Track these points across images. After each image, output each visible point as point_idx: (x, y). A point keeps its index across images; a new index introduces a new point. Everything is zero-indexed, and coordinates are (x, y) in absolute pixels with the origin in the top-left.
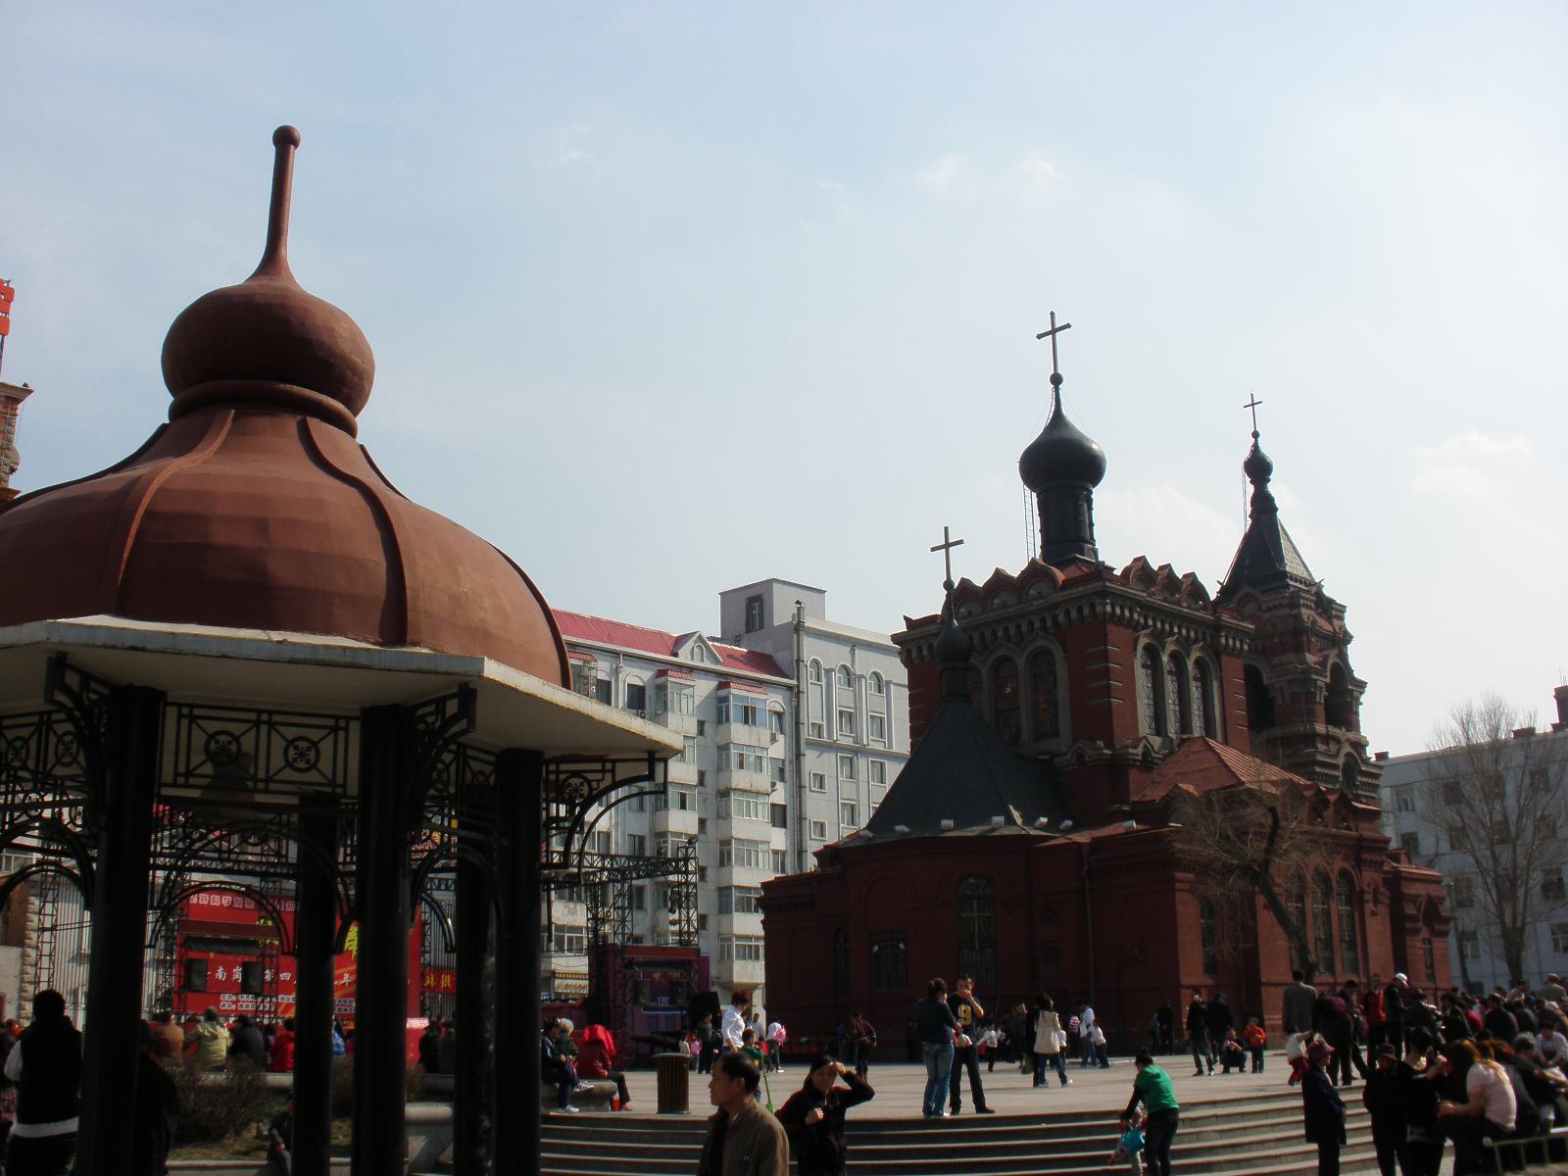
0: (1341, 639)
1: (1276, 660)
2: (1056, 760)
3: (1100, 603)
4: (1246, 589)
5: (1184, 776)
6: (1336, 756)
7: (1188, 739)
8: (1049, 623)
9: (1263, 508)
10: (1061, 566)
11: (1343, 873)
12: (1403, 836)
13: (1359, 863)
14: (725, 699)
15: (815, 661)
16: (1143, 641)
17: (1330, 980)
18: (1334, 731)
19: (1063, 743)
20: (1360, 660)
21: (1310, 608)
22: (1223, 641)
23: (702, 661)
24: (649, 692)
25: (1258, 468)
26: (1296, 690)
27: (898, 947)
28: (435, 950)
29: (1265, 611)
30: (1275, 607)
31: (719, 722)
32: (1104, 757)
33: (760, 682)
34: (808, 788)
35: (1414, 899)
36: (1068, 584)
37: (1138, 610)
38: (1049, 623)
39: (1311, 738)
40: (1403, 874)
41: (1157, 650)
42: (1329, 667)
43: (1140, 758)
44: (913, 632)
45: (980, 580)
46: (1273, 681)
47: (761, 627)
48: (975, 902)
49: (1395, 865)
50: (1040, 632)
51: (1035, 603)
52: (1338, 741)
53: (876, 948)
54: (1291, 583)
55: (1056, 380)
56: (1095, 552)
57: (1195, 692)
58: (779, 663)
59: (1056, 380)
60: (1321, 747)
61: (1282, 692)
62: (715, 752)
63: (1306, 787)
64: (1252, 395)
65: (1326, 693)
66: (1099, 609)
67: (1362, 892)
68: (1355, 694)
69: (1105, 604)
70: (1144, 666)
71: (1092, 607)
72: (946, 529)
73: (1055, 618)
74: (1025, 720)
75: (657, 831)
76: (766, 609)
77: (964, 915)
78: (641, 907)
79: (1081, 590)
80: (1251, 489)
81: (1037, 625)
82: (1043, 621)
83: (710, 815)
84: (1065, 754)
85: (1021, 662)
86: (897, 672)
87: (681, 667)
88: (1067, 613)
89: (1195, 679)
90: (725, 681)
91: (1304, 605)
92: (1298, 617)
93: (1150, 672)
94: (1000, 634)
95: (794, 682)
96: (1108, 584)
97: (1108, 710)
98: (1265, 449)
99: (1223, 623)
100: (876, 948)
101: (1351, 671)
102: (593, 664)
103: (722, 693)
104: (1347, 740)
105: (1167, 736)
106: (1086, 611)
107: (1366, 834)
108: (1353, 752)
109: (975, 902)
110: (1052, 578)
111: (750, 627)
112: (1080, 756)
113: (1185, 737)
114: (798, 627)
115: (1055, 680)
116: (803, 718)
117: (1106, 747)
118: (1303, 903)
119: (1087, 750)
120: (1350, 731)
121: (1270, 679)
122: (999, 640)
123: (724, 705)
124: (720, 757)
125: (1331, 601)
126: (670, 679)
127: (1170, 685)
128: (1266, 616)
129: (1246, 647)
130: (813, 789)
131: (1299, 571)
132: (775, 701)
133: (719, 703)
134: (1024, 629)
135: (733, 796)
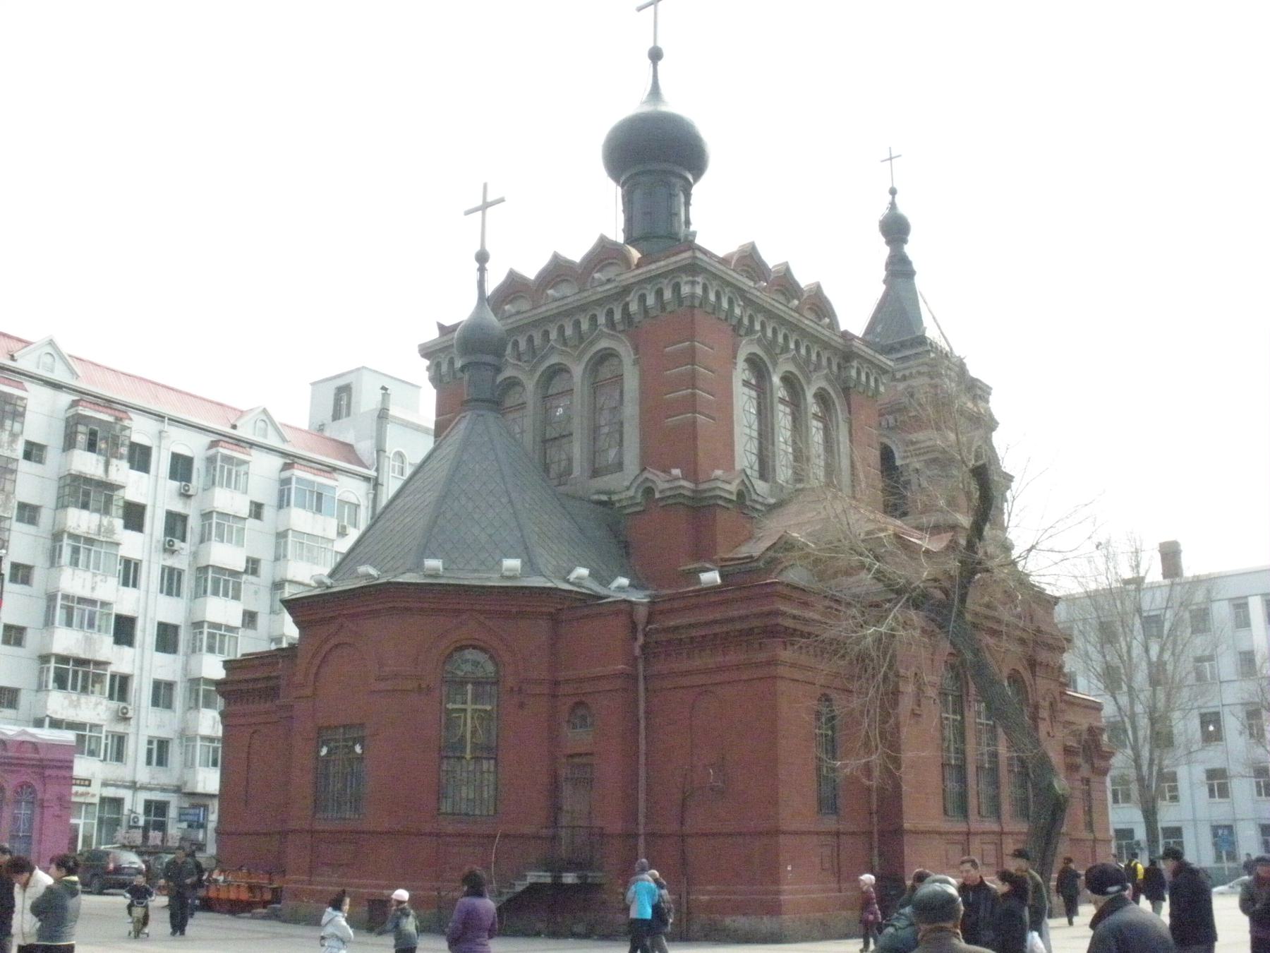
0: (986, 424)
1: (914, 437)
3: (686, 283)
5: (799, 526)
7: (802, 490)
8: (618, 316)
9: (899, 270)
14: (285, 482)
15: (400, 455)
16: (744, 351)
17: (995, 827)
25: (895, 229)
27: (352, 750)
29: (898, 380)
31: (280, 507)
33: (334, 469)
37: (741, 303)
38: (618, 316)
41: (767, 369)
43: (734, 498)
44: (445, 338)
45: (531, 271)
46: (908, 461)
47: (348, 414)
48: (469, 687)
50: (605, 330)
51: (600, 289)
53: (324, 751)
55: (656, 55)
58: (358, 453)
59: (656, 55)
62: (273, 540)
66: (686, 290)
69: (693, 283)
70: (746, 383)
71: (676, 288)
72: (485, 186)
74: (578, 450)
76: (354, 400)
77: (450, 706)
78: (169, 706)
80: (886, 251)
81: (602, 320)
82: (610, 313)
84: (628, 488)
85: (578, 370)
87: (239, 442)
95: (372, 473)
97: (691, 431)
98: (903, 209)
99: (855, 350)
100: (324, 751)
102: (126, 423)
103: (286, 474)
106: (668, 295)
110: (626, 259)
111: (336, 416)
112: (649, 492)
113: (799, 486)
114: (383, 415)
117: (685, 478)
121: (904, 458)
122: (552, 342)
124: (277, 545)
126: (221, 450)
128: (901, 386)
134: (585, 326)
135: (287, 584)
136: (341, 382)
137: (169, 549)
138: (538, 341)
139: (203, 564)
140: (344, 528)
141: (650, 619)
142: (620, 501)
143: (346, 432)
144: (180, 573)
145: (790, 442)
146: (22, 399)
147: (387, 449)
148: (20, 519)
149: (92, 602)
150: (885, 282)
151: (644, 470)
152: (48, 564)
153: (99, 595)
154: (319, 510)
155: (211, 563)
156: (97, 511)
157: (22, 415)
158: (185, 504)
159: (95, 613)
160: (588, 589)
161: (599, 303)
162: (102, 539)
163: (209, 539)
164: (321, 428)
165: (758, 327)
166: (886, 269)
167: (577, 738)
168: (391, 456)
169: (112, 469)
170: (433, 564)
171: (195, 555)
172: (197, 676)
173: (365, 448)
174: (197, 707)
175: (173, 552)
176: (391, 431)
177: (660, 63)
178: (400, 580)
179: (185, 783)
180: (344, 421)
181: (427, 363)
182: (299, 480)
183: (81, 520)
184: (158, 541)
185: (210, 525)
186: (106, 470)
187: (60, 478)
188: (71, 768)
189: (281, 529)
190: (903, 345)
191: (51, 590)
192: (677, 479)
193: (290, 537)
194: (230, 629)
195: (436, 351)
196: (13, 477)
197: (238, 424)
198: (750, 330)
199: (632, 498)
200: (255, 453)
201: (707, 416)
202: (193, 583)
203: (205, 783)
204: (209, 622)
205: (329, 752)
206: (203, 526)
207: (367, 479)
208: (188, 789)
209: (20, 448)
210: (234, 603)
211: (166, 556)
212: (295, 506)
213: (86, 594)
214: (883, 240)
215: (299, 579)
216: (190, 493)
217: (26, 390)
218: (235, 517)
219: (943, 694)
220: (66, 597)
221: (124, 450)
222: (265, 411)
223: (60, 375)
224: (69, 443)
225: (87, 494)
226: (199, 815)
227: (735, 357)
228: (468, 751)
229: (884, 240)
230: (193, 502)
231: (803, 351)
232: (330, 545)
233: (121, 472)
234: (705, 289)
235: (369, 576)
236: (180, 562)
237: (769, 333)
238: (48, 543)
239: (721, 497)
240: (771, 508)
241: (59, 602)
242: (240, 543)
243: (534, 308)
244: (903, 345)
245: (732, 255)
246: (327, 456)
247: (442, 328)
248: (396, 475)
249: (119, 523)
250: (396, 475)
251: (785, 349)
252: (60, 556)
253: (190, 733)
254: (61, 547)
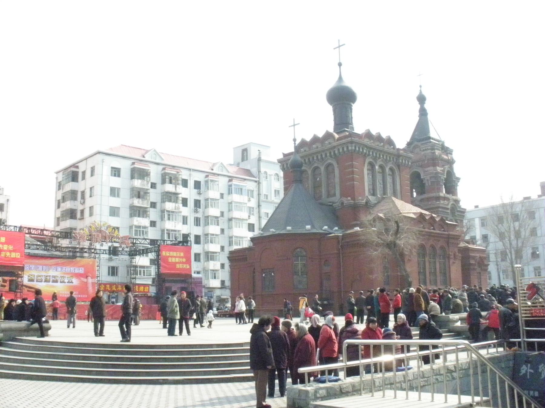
0: (451, 163)
1: (426, 169)
2: (334, 205)
4: (416, 143)
6: (448, 205)
7: (384, 198)
8: (332, 154)
9: (423, 113)
10: (338, 133)
11: (442, 248)
12: (483, 235)
13: (448, 243)
14: (230, 186)
15: (266, 173)
16: (367, 161)
18: (448, 196)
19: (337, 199)
20: (458, 170)
21: (439, 150)
22: (401, 161)
23: (219, 171)
24: (202, 184)
25: (421, 99)
26: (433, 180)
28: (101, 276)
30: (426, 150)
31: (229, 194)
32: (351, 204)
33: (245, 179)
34: (262, 218)
35: (474, 258)
36: (339, 139)
37: (366, 148)
38: (332, 154)
39: (438, 198)
40: (470, 249)
42: (446, 172)
43: (365, 204)
44: (285, 158)
45: (308, 139)
46: (425, 177)
47: (247, 159)
49: (467, 245)
50: (329, 157)
52: (448, 199)
53: (264, 275)
54: (432, 140)
55: (340, 65)
56: (353, 128)
57: (389, 180)
59: (340, 65)
60: (442, 202)
61: (428, 182)
62: (227, 204)
63: (428, 215)
65: (444, 182)
66: (350, 148)
67: (449, 255)
68: (456, 182)
69: (352, 146)
71: (348, 148)
72: (294, 119)
73: (334, 151)
75: (205, 233)
78: (199, 261)
79: (343, 141)
80: (419, 106)
82: (330, 153)
83: (225, 227)
85: (322, 168)
86: (281, 174)
87: (214, 174)
88: (339, 150)
89: (389, 175)
90: (231, 179)
91: (438, 149)
92: (434, 153)
93: (391, 177)
94: (315, 158)
95: (257, 179)
96: (353, 139)
98: (424, 93)
100: (264, 275)
101: (454, 174)
102: (180, 173)
103: (230, 183)
104: (452, 199)
105: (377, 196)
106: (345, 149)
107: (451, 233)
108: (454, 203)
109: (300, 258)
110: (333, 137)
111: (243, 160)
112: (342, 203)
113: (384, 196)
114: (259, 160)
115: (334, 175)
116: (261, 192)
118: (425, 259)
119: (344, 201)
120: (454, 196)
122: (315, 160)
123: (231, 188)
124: (229, 206)
125: (448, 148)
127: (379, 177)
128: (423, 153)
129: (410, 164)
130: (265, 218)
131: (437, 137)
132: (251, 185)
133: (229, 187)
134: (324, 156)
135: (233, 219)
136: (244, 148)
137: (196, 211)
138: (311, 160)
139: (206, 215)
140: (249, 199)
141: (342, 240)
142: (335, 206)
143: (246, 165)
144: (200, 219)
145: (382, 183)
146: (149, 170)
147: (262, 171)
148: (151, 207)
149: (175, 231)
150: (419, 116)
151: (341, 198)
152: (160, 220)
153: (177, 229)
154: (242, 194)
155: (210, 215)
156: (174, 202)
157: (149, 175)
158: (200, 196)
159: (176, 234)
160: (328, 231)
161: (327, 150)
162: (176, 211)
163: (208, 207)
164: (238, 165)
165: (371, 153)
166: (419, 112)
167: (326, 269)
168: (263, 173)
169: (177, 189)
170: (289, 228)
171: (204, 213)
172: (207, 251)
173: (254, 171)
174: (208, 260)
175: (197, 212)
176: (262, 164)
177: (341, 67)
178: (281, 233)
179: (206, 284)
180: (245, 162)
181: (280, 164)
182: (234, 185)
183: (169, 206)
184: (192, 209)
185: (208, 202)
186: (176, 189)
187: (162, 193)
188: (202, 283)
189: (230, 201)
190: (423, 140)
191: (162, 228)
192: (349, 200)
193: (233, 204)
194: (217, 235)
195: (282, 162)
196: (149, 195)
197: (214, 169)
198: (369, 155)
199: (339, 205)
200: (220, 177)
201: (357, 182)
202: (204, 222)
203: (212, 284)
204: (210, 234)
205: (265, 275)
206: (206, 203)
207: (256, 181)
208: (207, 286)
209: (150, 185)
210: (218, 226)
211: (195, 213)
212: (234, 193)
213: (173, 228)
214: (418, 103)
215: (237, 217)
216: (201, 193)
217: (150, 167)
218: (215, 199)
219: (419, 254)
220: (167, 230)
221: (180, 182)
222: (222, 163)
223: (158, 161)
224: (163, 182)
225: (170, 197)
226: (211, 294)
227: (364, 164)
228: (300, 273)
229: (418, 103)
230: (202, 196)
231: (385, 157)
232: (246, 205)
233: (180, 189)
234: (355, 147)
235: (272, 231)
236: (199, 215)
237: (374, 155)
238: (160, 214)
239: (360, 204)
240: (376, 205)
241: (166, 232)
242: (218, 207)
243: (309, 150)
244: (423, 140)
245: (363, 134)
246: (242, 175)
247: (283, 154)
248: (265, 179)
249: (181, 205)
250: (265, 179)
251: (379, 158)
252: (164, 217)
253: (206, 269)
254: (164, 215)
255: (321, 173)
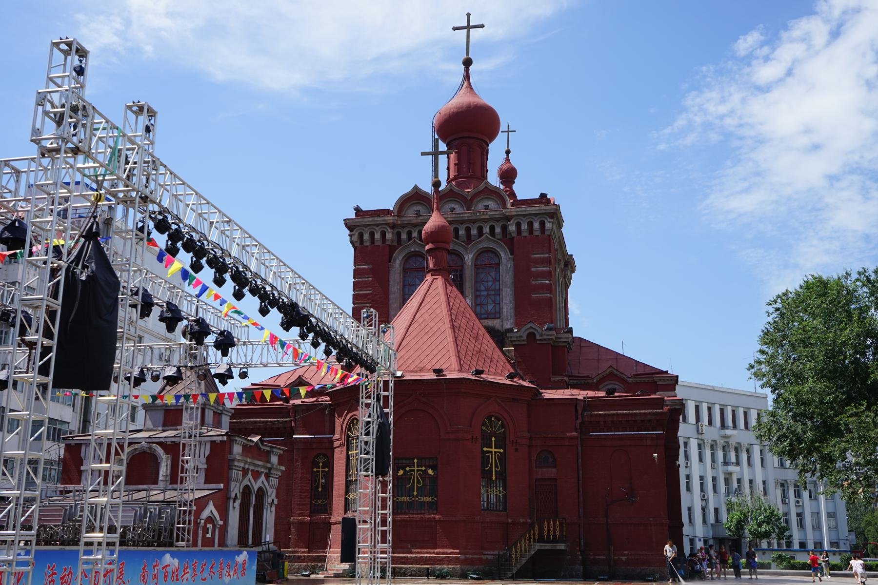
3: (549, 222)
64: (509, 125)
71: (542, 224)
81: (486, 230)
88: (519, 225)
98: (514, 162)
112: (531, 336)
142: (511, 337)
161: (486, 221)
199: (521, 337)
247: (358, 210)
255: (498, 264)
